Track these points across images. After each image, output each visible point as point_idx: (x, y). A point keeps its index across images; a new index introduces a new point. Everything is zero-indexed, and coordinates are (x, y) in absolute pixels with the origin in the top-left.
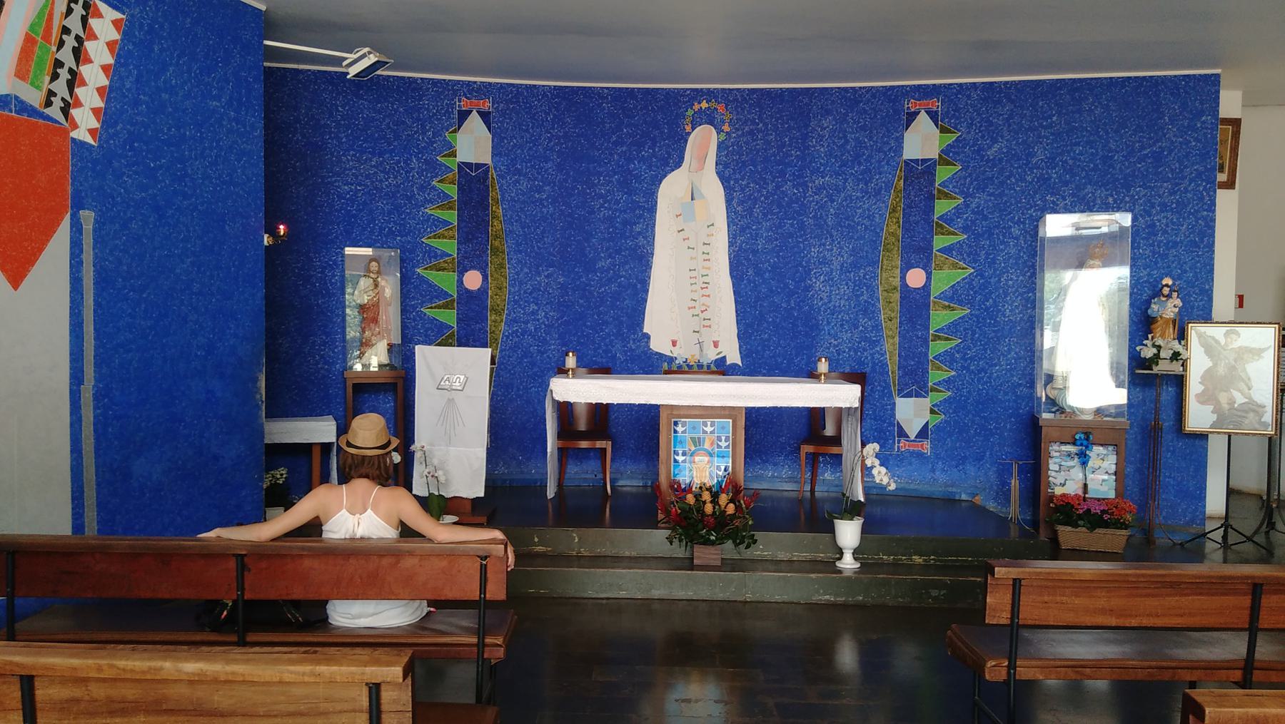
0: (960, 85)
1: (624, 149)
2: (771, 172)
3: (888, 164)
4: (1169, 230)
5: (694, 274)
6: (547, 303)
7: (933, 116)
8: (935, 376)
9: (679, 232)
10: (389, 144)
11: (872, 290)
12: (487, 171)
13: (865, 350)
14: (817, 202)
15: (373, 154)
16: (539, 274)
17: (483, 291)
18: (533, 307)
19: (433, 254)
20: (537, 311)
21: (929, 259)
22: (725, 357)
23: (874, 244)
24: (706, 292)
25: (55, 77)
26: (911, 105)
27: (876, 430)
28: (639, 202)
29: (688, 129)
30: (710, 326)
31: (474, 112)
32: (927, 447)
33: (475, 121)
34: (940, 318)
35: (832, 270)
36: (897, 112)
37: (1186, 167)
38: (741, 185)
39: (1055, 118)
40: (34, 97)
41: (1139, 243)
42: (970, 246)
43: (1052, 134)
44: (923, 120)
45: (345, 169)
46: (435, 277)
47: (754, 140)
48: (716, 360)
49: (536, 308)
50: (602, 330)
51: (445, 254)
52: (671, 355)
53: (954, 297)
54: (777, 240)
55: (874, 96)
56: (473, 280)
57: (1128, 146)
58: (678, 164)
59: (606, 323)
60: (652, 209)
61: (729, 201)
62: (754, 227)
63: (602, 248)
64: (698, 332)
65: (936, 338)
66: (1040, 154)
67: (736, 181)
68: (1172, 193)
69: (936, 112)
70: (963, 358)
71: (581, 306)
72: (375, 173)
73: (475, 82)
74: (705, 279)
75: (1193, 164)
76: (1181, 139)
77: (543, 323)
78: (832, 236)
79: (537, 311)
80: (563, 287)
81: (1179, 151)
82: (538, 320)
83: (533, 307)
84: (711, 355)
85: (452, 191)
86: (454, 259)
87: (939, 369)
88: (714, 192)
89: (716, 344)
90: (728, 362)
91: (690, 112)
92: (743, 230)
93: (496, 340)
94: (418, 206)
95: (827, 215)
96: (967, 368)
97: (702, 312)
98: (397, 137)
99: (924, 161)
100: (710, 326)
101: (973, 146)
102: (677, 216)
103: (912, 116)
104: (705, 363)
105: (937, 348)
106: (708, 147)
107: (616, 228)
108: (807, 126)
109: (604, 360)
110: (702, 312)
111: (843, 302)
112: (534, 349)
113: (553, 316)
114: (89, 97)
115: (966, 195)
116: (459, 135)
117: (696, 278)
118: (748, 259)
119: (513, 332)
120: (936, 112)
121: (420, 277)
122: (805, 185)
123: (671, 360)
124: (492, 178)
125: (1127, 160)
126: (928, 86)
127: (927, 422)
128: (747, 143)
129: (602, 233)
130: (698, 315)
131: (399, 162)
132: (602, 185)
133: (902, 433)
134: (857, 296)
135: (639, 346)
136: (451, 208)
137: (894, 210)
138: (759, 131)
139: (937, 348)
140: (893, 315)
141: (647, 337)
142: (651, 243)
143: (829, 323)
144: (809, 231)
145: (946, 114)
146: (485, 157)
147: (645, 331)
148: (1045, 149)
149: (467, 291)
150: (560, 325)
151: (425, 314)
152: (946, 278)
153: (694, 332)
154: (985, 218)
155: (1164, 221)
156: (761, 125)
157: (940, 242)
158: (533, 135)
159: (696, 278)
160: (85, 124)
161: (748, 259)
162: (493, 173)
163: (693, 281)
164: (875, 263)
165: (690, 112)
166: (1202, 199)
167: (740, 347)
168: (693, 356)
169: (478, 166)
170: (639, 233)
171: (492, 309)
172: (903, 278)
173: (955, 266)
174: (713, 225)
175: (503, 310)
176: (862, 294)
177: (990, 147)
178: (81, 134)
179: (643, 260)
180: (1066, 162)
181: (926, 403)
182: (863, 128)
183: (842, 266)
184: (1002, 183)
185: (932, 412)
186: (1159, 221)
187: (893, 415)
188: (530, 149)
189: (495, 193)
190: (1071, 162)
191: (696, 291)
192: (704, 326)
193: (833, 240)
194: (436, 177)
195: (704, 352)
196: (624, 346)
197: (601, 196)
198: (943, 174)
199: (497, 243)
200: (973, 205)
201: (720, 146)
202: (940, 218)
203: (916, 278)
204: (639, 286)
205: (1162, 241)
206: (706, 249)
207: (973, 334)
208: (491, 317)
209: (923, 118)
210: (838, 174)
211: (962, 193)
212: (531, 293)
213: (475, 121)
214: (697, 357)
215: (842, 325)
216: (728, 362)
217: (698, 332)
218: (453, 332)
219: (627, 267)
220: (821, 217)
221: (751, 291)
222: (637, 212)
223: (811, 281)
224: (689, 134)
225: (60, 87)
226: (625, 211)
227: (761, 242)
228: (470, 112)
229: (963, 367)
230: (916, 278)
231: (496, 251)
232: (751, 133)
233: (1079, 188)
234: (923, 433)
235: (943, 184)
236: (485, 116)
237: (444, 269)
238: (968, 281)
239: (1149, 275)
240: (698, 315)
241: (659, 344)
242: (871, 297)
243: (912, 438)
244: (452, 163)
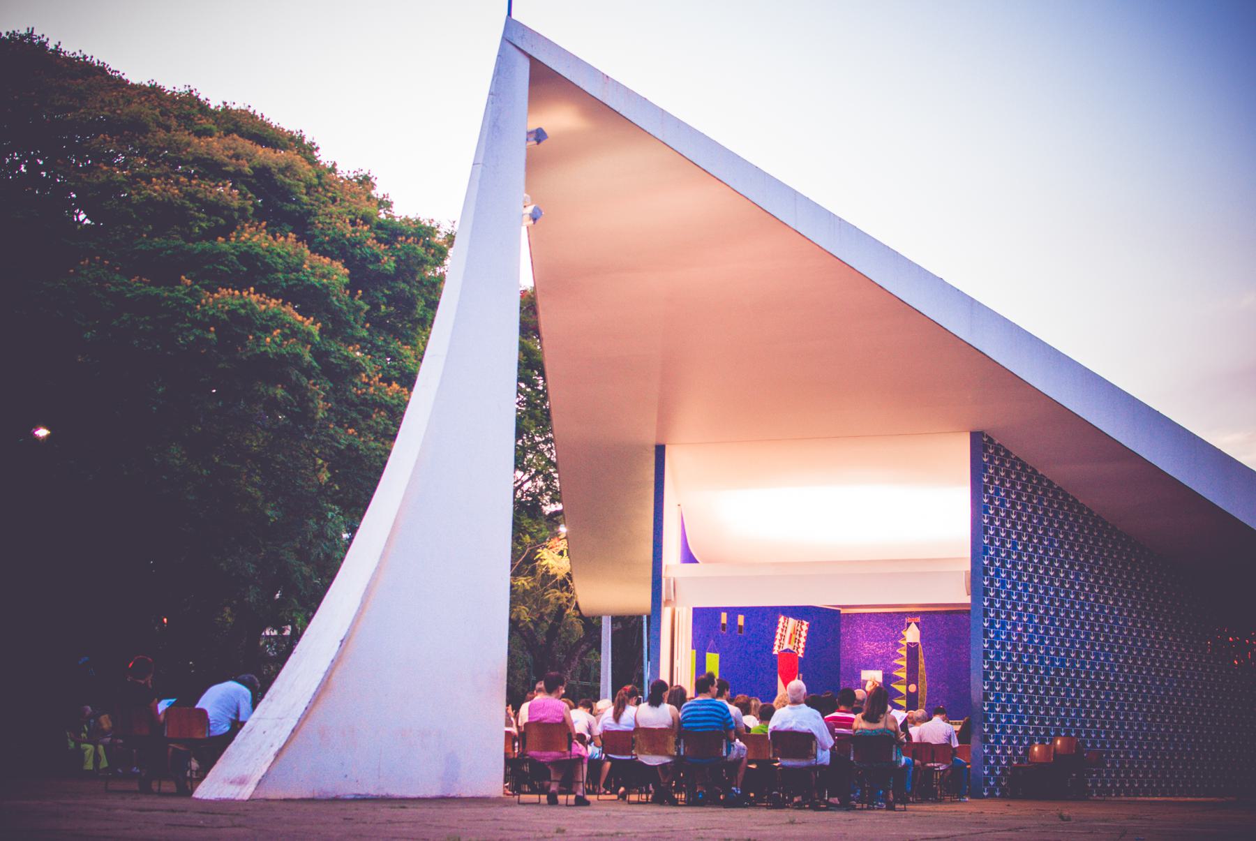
10: (881, 637)
12: (918, 645)
15: (875, 641)
17: (917, 692)
18: (937, 698)
19: (897, 679)
25: (795, 642)
33: (913, 626)
40: (791, 647)
51: (902, 678)
56: (912, 688)
85: (904, 653)
98: (884, 634)
114: (802, 645)
116: (907, 632)
136: (904, 660)
146: (918, 640)
160: (801, 653)
169: (915, 643)
178: (800, 655)
189: (921, 654)
225: (796, 644)
228: (911, 623)
236: (917, 624)
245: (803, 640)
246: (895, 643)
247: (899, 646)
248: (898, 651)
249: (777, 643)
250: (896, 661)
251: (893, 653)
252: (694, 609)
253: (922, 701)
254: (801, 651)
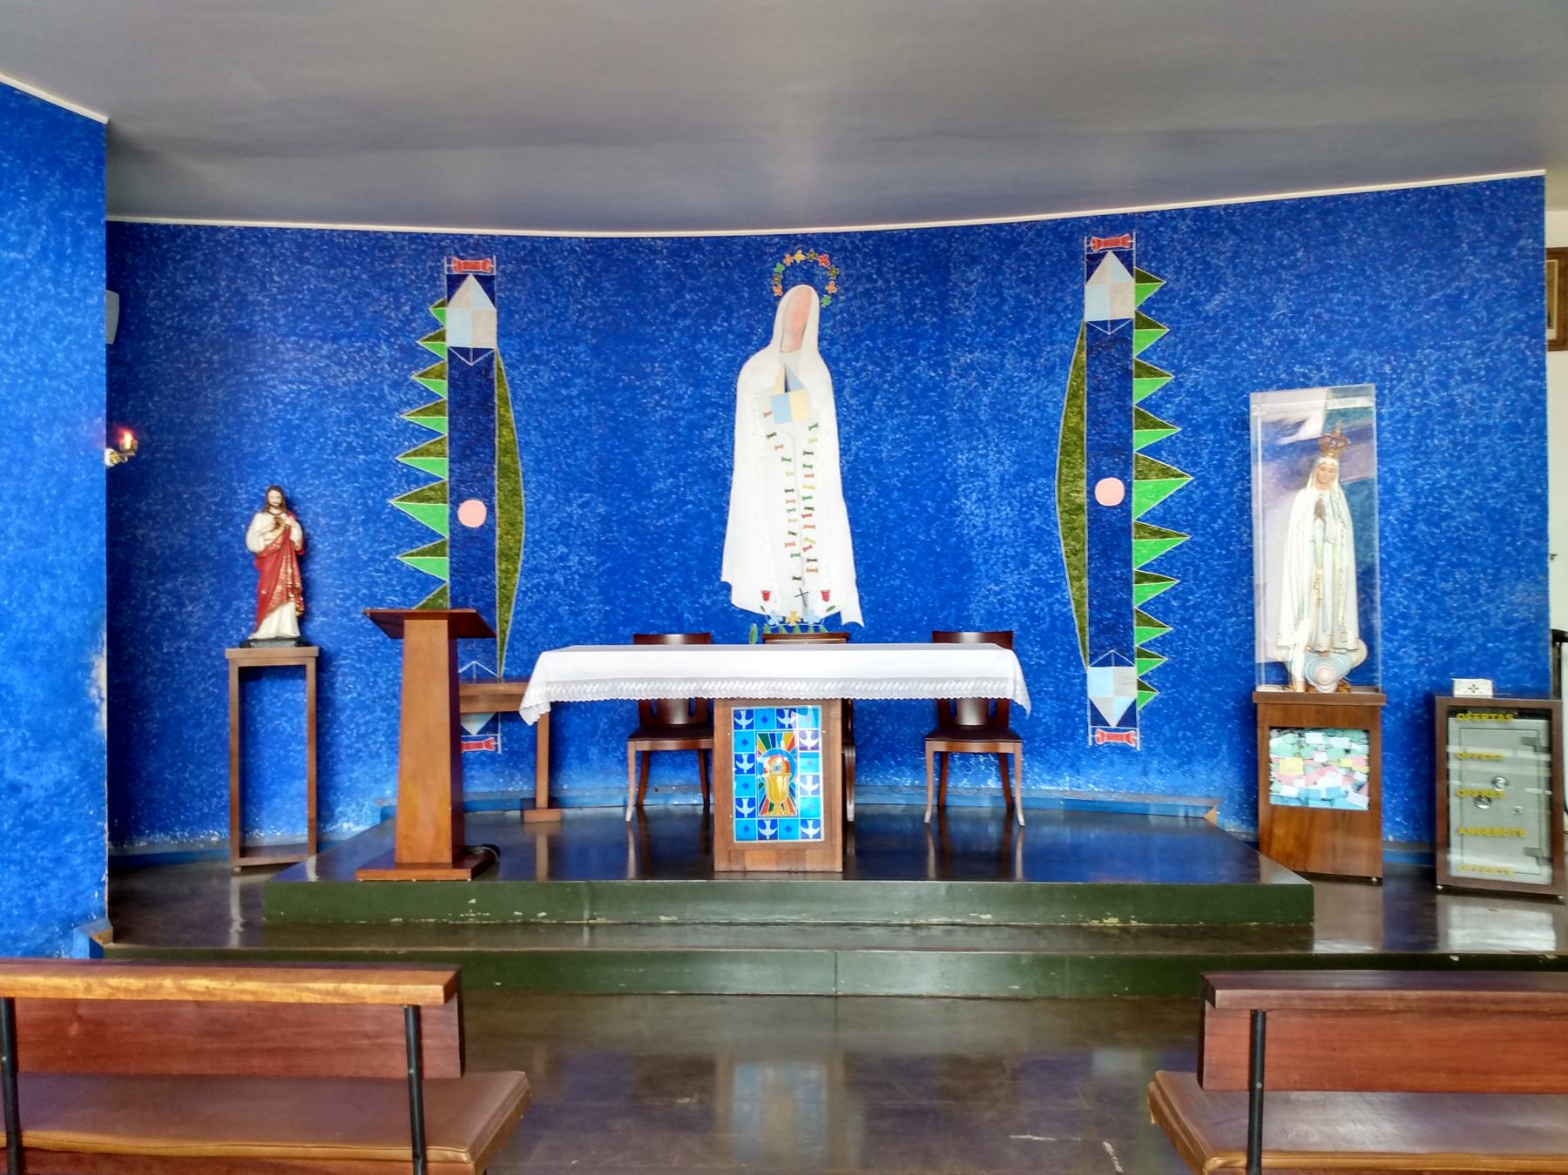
0: (1162, 213)
1: (688, 322)
2: (898, 348)
3: (1063, 329)
4: (1476, 408)
5: (791, 496)
6: (582, 544)
7: (1125, 257)
8: (1143, 635)
9: (769, 436)
10: (348, 325)
11: (1046, 510)
12: (490, 360)
13: (1039, 598)
14: (964, 388)
15: (324, 339)
16: (569, 502)
17: (488, 528)
18: (562, 549)
19: (413, 477)
20: (568, 555)
21: (1128, 464)
22: (838, 614)
23: (1048, 444)
24: (808, 521)
26: (1092, 244)
27: (1059, 715)
28: (710, 397)
29: (777, 291)
30: (816, 570)
31: (471, 279)
32: (1135, 738)
33: (471, 290)
34: (1145, 551)
35: (988, 485)
36: (1074, 255)
37: (1498, 315)
38: (854, 368)
39: (1300, 254)
41: (1433, 430)
42: (1187, 444)
43: (1298, 277)
44: (1111, 266)
45: (284, 362)
46: (414, 510)
47: (871, 304)
48: (827, 619)
49: (566, 550)
50: (662, 580)
51: (431, 478)
52: (761, 612)
53: (1164, 518)
54: (907, 443)
55: (1039, 234)
56: (473, 513)
57: (1409, 289)
58: (765, 341)
59: (668, 569)
60: (730, 407)
61: (838, 391)
62: (875, 427)
63: (659, 463)
64: (799, 579)
65: (1142, 578)
66: (1281, 307)
67: (848, 362)
68: (1479, 354)
69: (1129, 254)
70: (1183, 607)
71: (631, 545)
72: (327, 365)
73: (471, 236)
74: (809, 503)
75: (1508, 310)
76: (1488, 276)
77: (577, 572)
78: (986, 436)
79: (568, 555)
80: (605, 520)
81: (1486, 292)
82: (569, 568)
83: (562, 549)
84: (819, 611)
85: (441, 388)
86: (444, 484)
87: (1149, 623)
89: (826, 596)
90: (845, 621)
91: (779, 268)
92: (859, 431)
93: (508, 598)
94: (391, 411)
95: (978, 406)
96: (1189, 621)
97: (805, 549)
98: (358, 314)
99: (1115, 323)
100: (816, 570)
101: (1184, 299)
102: (765, 415)
103: (1095, 260)
104: (811, 624)
105: (1144, 593)
106: (806, 317)
107: (680, 434)
108: (945, 280)
109: (666, 623)
110: (805, 549)
111: (1005, 530)
112: (564, 610)
113: (591, 562)
115: (1178, 370)
117: (794, 501)
118: (867, 473)
119: (534, 586)
120: (1129, 254)
121: (397, 513)
122: (945, 365)
123: (762, 619)
124: (500, 369)
125: (1409, 309)
126: (1115, 216)
127: (1134, 704)
128: (861, 308)
129: (659, 442)
130: (798, 555)
131: (361, 350)
132: (657, 374)
133: (1098, 719)
134: (1026, 521)
135: (714, 603)
136: (439, 413)
137: (1074, 396)
138: (878, 290)
139: (1144, 593)
140: (1078, 546)
141: (727, 587)
142: (730, 455)
143: (986, 561)
144: (953, 429)
145: (1143, 256)
147: (723, 579)
148: (1288, 299)
149: (465, 529)
150: (601, 574)
151: (402, 564)
152: (1151, 493)
153: (795, 578)
154: (1206, 401)
155: (1469, 396)
156: (880, 282)
157: (1142, 439)
158: (556, 307)
159: (794, 501)
161: (867, 473)
162: (499, 362)
163: (791, 506)
164: (1049, 473)
165: (779, 268)
166: (1524, 361)
167: (861, 598)
168: (793, 613)
169: (478, 352)
170: (712, 441)
171: (502, 554)
172: (1091, 492)
173: (1165, 473)
174: (816, 426)
175: (518, 555)
176: (1033, 517)
177: (1208, 300)
179: (718, 478)
180: (1319, 316)
181: (1131, 673)
182: (1026, 280)
183: (1002, 478)
184: (1229, 350)
185: (1141, 686)
186: (1461, 396)
187: (1084, 692)
188: (553, 326)
189: (501, 390)
190: (1326, 316)
191: (795, 521)
192: (808, 570)
193: (988, 442)
194: (416, 369)
195: (810, 607)
196: (696, 602)
197: (656, 390)
198: (1143, 340)
199: (507, 460)
200: (1189, 384)
201: (824, 314)
202: (1141, 404)
203: (1109, 492)
204: (714, 515)
205: (1465, 426)
206: (808, 460)
207: (1196, 572)
208: (500, 565)
209: (1111, 263)
210: (990, 347)
211: (1171, 366)
212: (558, 530)
213: (471, 288)
214: (799, 615)
215: (1005, 564)
216: (845, 621)
217: (799, 579)
218: (445, 589)
219: (696, 489)
220: (970, 410)
221: (873, 517)
222: (708, 411)
223: (958, 500)
224: (779, 298)
226: (690, 410)
227: (885, 448)
228: (463, 277)
229: (1183, 620)
230: (1109, 492)
231: (506, 472)
232: (867, 293)
233: (1341, 353)
234: (1129, 718)
235: (1143, 355)
236: (486, 282)
237: (429, 500)
238: (1186, 494)
239: (1451, 476)
240: (798, 555)
241: (746, 598)
242: (1046, 521)
243: (1113, 724)
244: (440, 349)
246: (402, 348)
247: (413, 357)
248: (414, 377)
250: (408, 416)
251: (395, 386)
253: (508, 556)
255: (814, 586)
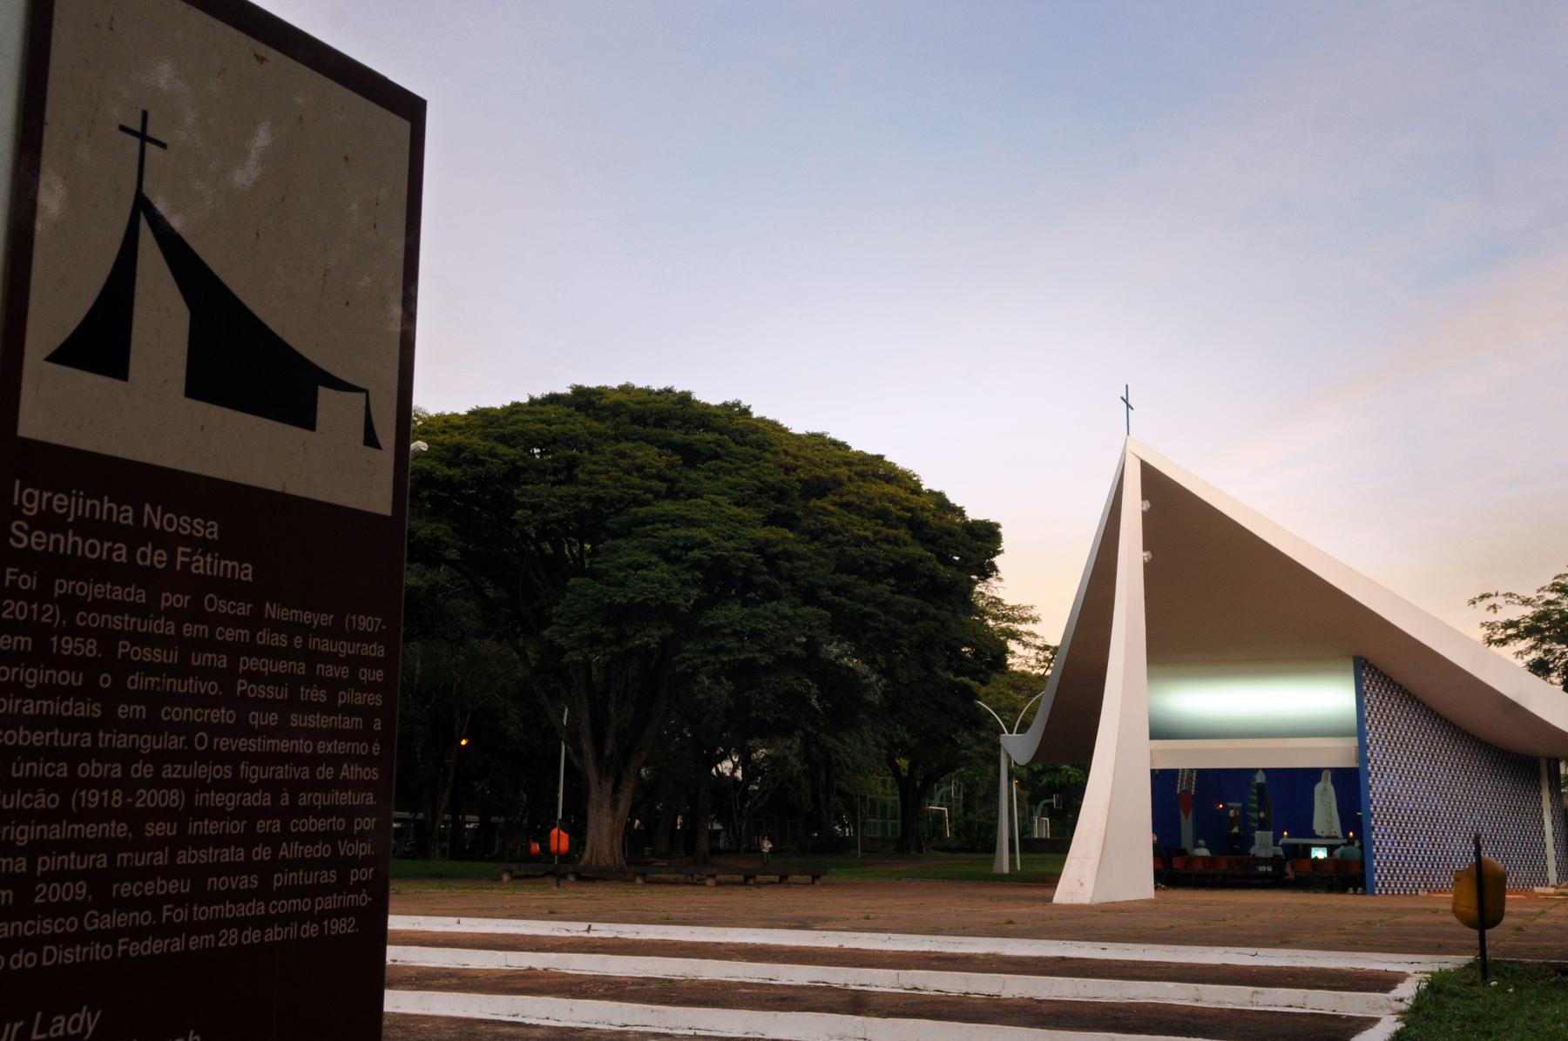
17: (1265, 817)
56: (1262, 815)
58: (1320, 780)
85: (1255, 791)
88: (1331, 788)
114: (1193, 787)
241: (1318, 832)
245: (1194, 783)
249: (1179, 785)
252: (1153, 771)
254: (1193, 790)
255: (1333, 830)
